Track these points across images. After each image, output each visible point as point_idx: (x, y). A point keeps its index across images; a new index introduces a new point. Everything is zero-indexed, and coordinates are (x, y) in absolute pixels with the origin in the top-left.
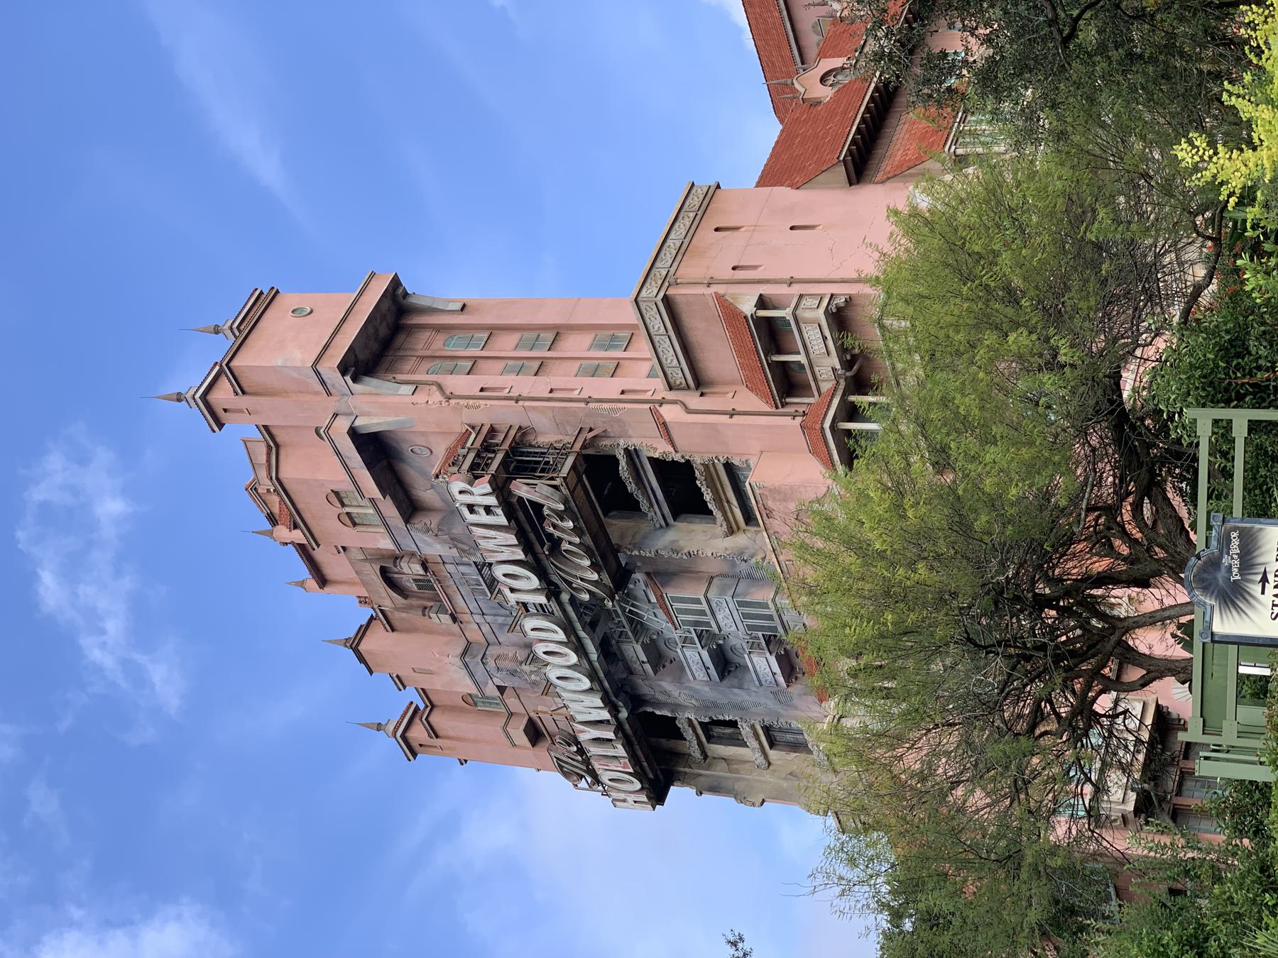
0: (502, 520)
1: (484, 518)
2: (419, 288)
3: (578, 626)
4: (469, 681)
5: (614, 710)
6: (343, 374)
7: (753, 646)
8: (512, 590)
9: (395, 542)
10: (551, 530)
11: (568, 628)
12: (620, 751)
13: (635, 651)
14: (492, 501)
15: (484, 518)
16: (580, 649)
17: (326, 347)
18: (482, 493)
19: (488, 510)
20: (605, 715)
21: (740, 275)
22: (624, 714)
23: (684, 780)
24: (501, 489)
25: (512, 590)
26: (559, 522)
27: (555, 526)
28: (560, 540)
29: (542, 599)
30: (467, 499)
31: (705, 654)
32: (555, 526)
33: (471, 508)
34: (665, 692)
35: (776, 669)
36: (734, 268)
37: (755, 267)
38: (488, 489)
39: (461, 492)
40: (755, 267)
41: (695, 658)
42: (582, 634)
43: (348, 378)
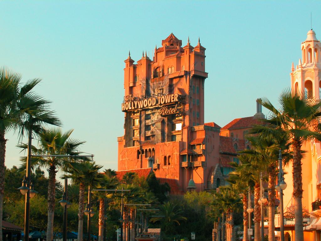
0: (172, 101)
1: (172, 98)
2: (206, 80)
3: (155, 107)
4: (142, 79)
5: (140, 109)
6: (193, 75)
7: (152, 132)
8: (160, 99)
9: (166, 75)
10: (171, 109)
11: (155, 105)
12: (133, 108)
13: (149, 112)
14: (175, 101)
15: (172, 98)
16: (152, 106)
17: (197, 71)
18: (176, 99)
19: (173, 99)
20: (140, 107)
21: (207, 140)
22: (139, 110)
23: (127, 115)
24: (176, 102)
25: (160, 99)
26: (172, 111)
27: (171, 110)
28: (169, 110)
29: (159, 103)
30: (175, 96)
31: (150, 124)
32: (171, 110)
33: (173, 96)
34: (143, 115)
35: (148, 135)
36: (208, 139)
37: (208, 142)
38: (177, 100)
39: (176, 96)
40: (208, 142)
41: (149, 122)
42: (153, 107)
43: (192, 75)
